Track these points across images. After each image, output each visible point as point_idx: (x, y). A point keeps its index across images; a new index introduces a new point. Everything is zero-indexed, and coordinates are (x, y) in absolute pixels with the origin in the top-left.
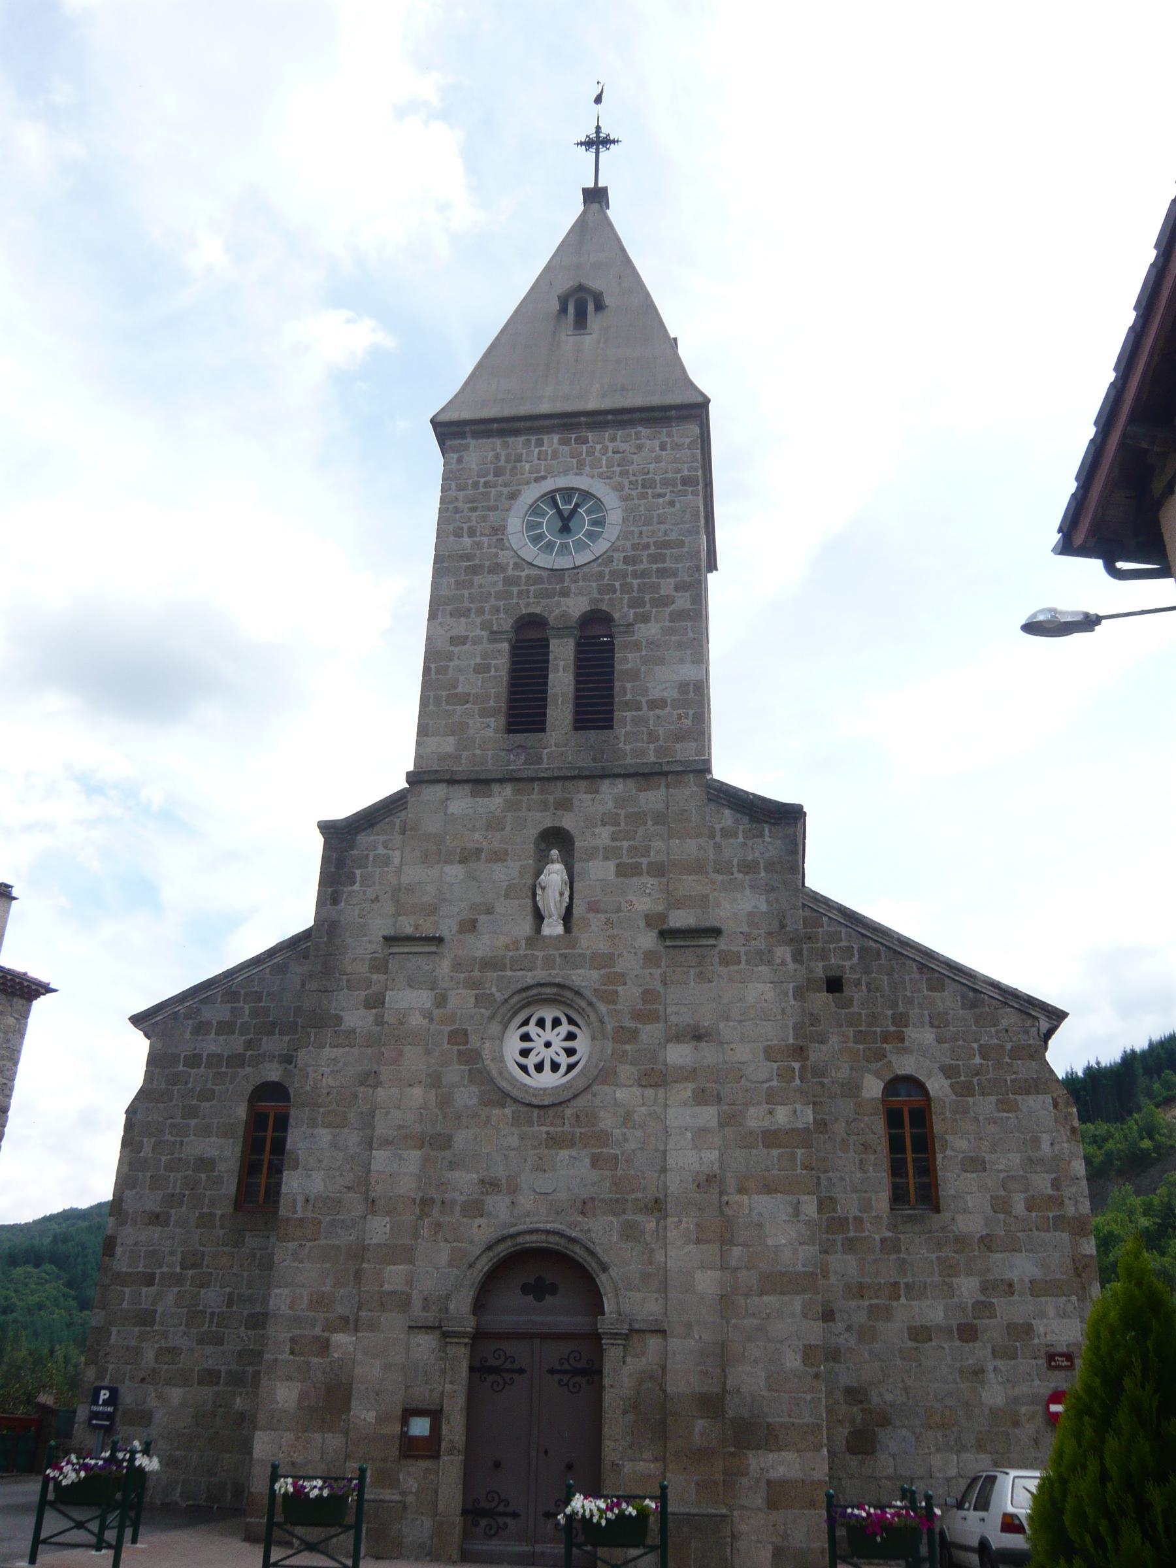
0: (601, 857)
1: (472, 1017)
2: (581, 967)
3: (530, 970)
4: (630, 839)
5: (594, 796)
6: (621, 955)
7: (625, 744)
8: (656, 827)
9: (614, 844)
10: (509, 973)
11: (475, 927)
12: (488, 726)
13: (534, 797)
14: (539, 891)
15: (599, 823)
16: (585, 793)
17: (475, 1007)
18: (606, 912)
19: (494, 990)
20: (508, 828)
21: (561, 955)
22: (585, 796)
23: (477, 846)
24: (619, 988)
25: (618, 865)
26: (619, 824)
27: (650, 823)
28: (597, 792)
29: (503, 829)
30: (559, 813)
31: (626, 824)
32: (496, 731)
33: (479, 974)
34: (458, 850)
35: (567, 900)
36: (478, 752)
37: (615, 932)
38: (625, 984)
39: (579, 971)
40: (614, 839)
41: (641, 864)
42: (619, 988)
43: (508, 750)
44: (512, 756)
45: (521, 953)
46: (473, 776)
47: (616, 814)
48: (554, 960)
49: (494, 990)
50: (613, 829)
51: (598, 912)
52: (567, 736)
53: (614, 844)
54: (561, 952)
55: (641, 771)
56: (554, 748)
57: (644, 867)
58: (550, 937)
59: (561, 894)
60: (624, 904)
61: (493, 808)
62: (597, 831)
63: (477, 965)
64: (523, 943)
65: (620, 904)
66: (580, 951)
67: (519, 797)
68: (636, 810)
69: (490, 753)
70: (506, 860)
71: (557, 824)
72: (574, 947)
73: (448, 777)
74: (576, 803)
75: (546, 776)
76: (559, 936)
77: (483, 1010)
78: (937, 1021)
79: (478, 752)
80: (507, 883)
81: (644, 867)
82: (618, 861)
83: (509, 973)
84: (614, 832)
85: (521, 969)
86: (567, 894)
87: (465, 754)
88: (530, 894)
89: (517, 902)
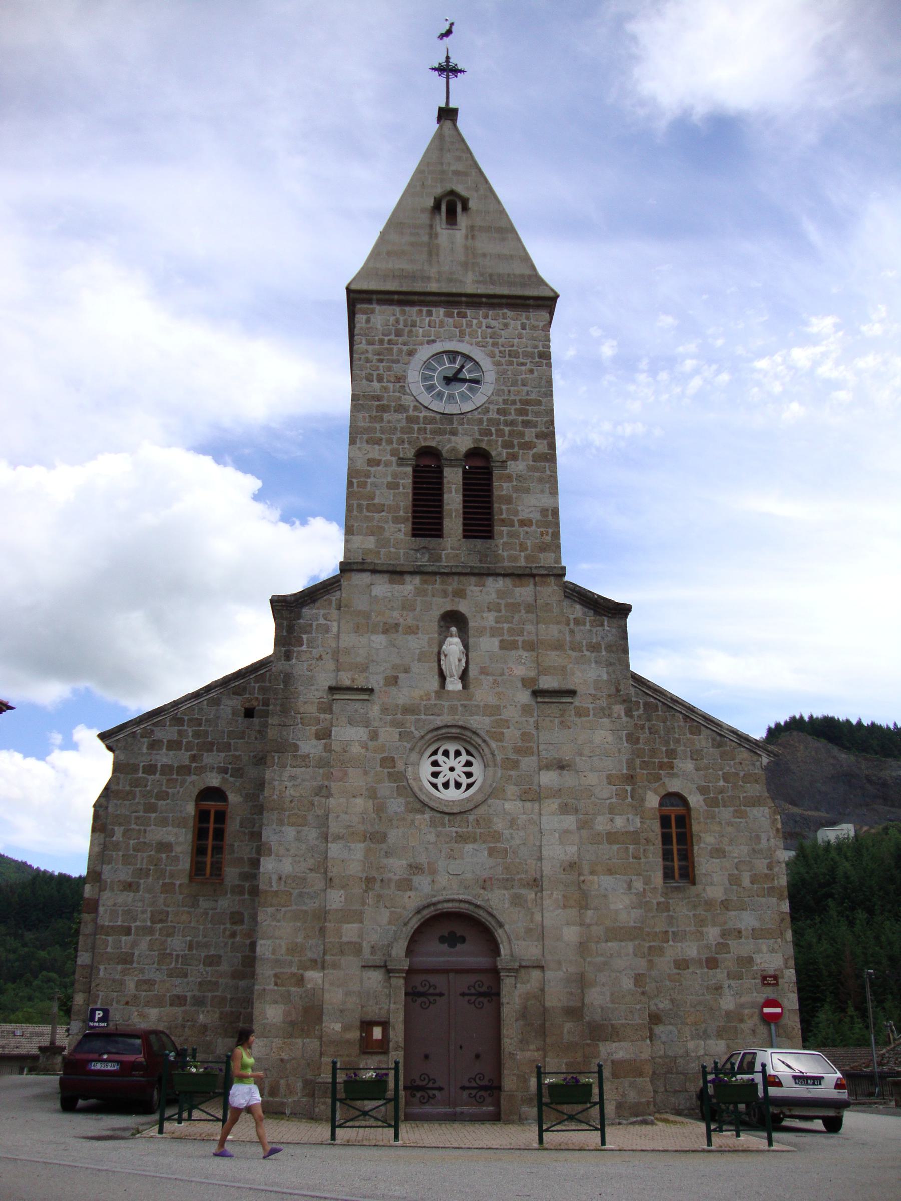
0: (488, 634)
1: (398, 748)
2: (478, 715)
3: (439, 715)
4: (509, 622)
5: (480, 588)
6: (505, 707)
7: (503, 551)
8: (527, 615)
9: (497, 625)
10: (423, 717)
11: (397, 682)
12: (400, 531)
13: (437, 586)
14: (443, 657)
15: (486, 609)
16: (475, 586)
17: (400, 741)
18: (493, 675)
19: (413, 729)
20: (418, 609)
21: (462, 705)
22: (475, 588)
23: (397, 621)
24: (505, 731)
25: (501, 641)
26: (500, 611)
27: (523, 611)
28: (483, 586)
29: (415, 609)
30: (456, 600)
31: (506, 611)
32: (406, 534)
33: (401, 716)
34: (382, 624)
35: (464, 665)
36: (393, 550)
37: (500, 689)
38: (508, 727)
39: (475, 717)
40: (496, 622)
41: (517, 641)
42: (505, 731)
43: (415, 550)
44: (419, 555)
45: (433, 702)
46: (391, 569)
47: (498, 603)
48: (456, 708)
49: (413, 729)
50: (496, 614)
51: (487, 674)
52: (459, 543)
53: (497, 625)
54: (462, 702)
55: (516, 572)
56: (450, 551)
57: (520, 643)
58: (453, 691)
59: (459, 660)
60: (506, 670)
61: (406, 593)
62: (485, 615)
63: (400, 710)
64: (433, 694)
65: (503, 669)
66: (476, 703)
67: (426, 586)
68: (512, 601)
69: (402, 551)
70: (417, 633)
71: (454, 608)
72: (470, 699)
73: (371, 568)
74: (468, 593)
75: (446, 571)
76: (459, 691)
77: (405, 743)
78: (696, 755)
79: (393, 550)
80: (419, 650)
81: (520, 643)
82: (501, 638)
83: (423, 717)
84: (496, 617)
85: (433, 714)
86: (463, 661)
87: (383, 551)
88: (436, 659)
89: (427, 664)
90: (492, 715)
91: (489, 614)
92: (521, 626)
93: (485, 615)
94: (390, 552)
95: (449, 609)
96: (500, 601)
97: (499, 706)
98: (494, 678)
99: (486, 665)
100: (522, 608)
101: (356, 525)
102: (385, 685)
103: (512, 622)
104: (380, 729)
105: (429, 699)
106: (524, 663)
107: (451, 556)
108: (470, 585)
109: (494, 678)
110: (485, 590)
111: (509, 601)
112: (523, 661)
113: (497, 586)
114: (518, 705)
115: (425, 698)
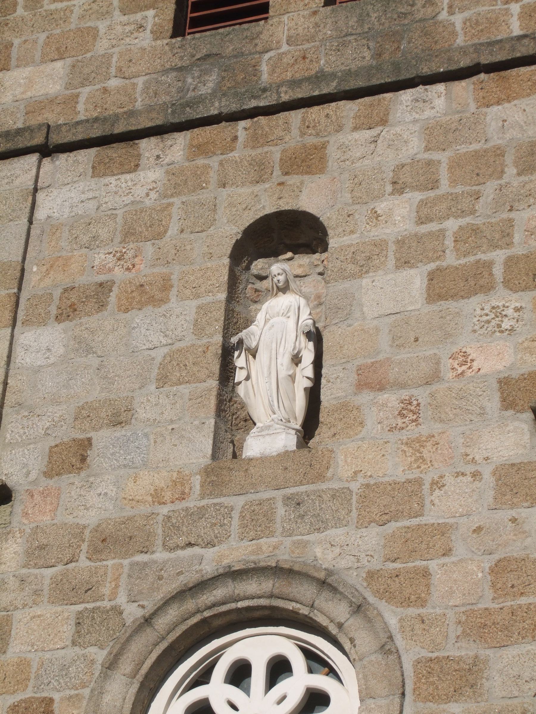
0: (391, 262)
3: (210, 544)
4: (463, 213)
6: (437, 484)
7: (451, 13)
9: (424, 229)
10: (161, 555)
11: (83, 459)
12: (141, 27)
13: (235, 155)
15: (389, 188)
17: (74, 643)
18: (403, 386)
19: (122, 599)
20: (173, 230)
21: (287, 499)
22: (356, 135)
26: (434, 184)
27: (511, 171)
28: (384, 122)
30: (293, 180)
31: (453, 182)
32: (156, 35)
33: (88, 563)
34: (57, 293)
35: (310, 372)
36: (114, 83)
37: (424, 429)
38: (447, 552)
39: (332, 533)
40: (420, 221)
41: (489, 265)
43: (180, 69)
44: (190, 80)
45: (191, 503)
46: (96, 132)
47: (429, 163)
49: (122, 599)
51: (381, 388)
53: (424, 229)
54: (290, 491)
55: (485, 59)
56: (285, 48)
57: (498, 271)
58: (263, 460)
59: (296, 360)
62: (381, 207)
63: (84, 547)
64: (197, 480)
66: (336, 485)
67: (201, 161)
68: (475, 146)
69: (140, 81)
71: (286, 205)
72: (321, 477)
74: (332, 152)
75: (262, 104)
76: (285, 455)
77: (93, 650)
79: (114, 83)
81: (498, 271)
82: (432, 266)
83: (161, 555)
84: (422, 203)
85: (190, 544)
86: (308, 357)
87: (85, 91)
89: (185, 390)
90: (395, 518)
91: (397, 200)
92: (505, 215)
93: (381, 207)
94: (105, 90)
95: (270, 209)
96: (435, 156)
97: (419, 482)
98: (405, 394)
99: (381, 357)
100: (509, 159)
101: (16, 42)
102: (48, 474)
103: (473, 212)
104: (18, 615)
105: (183, 497)
106: (512, 330)
107: (286, 60)
108: (340, 129)
109: (405, 394)
110: (387, 133)
111: (463, 149)
112: (506, 325)
113: (428, 113)
114: (487, 472)
115: (168, 495)
